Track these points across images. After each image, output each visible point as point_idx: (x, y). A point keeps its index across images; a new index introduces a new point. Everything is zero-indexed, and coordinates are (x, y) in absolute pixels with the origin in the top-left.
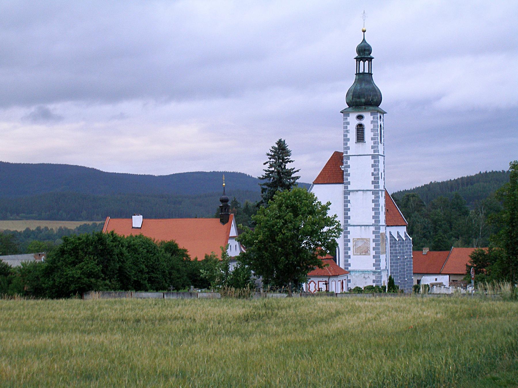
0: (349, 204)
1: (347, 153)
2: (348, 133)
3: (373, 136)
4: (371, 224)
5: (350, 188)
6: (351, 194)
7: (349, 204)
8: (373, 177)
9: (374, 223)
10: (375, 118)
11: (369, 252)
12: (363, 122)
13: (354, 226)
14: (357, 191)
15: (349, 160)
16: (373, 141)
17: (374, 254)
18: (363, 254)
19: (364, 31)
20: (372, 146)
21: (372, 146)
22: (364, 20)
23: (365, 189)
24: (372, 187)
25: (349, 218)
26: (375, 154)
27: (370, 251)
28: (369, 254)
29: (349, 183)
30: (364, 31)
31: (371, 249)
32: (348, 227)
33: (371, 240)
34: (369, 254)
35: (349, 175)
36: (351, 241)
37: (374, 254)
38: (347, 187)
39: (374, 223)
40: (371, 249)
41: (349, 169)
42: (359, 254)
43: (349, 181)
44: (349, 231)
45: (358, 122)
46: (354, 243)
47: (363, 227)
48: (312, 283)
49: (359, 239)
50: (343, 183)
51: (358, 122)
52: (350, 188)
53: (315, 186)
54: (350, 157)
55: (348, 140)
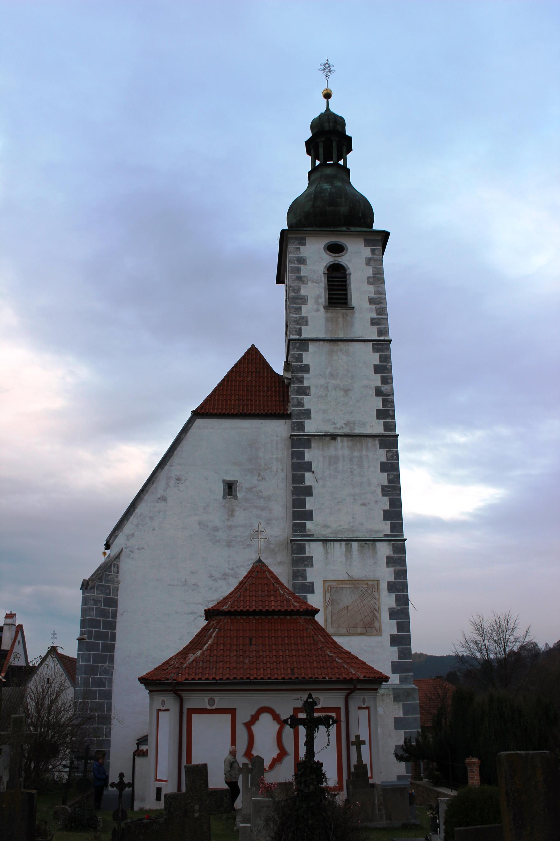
0: (308, 475)
1: (300, 334)
2: (304, 283)
3: (373, 295)
4: (381, 536)
5: (310, 427)
6: (313, 445)
7: (308, 475)
8: (380, 399)
9: (388, 532)
10: (377, 252)
11: (377, 624)
12: (344, 260)
13: (325, 541)
14: (333, 437)
15: (307, 350)
16: (374, 307)
17: (395, 632)
18: (359, 630)
19: (327, 96)
20: (372, 319)
21: (372, 319)
22: (327, 76)
23: (358, 430)
24: (378, 428)
25: (309, 515)
26: (382, 338)
27: (379, 620)
28: (379, 633)
29: (307, 414)
30: (327, 96)
31: (385, 615)
32: (307, 544)
33: (384, 586)
34: (379, 633)
35: (305, 391)
36: (319, 588)
37: (395, 632)
38: (301, 426)
39: (388, 532)
40: (385, 615)
41: (305, 375)
42: (344, 631)
43: (306, 407)
44: (311, 558)
45: (328, 259)
46: (328, 595)
47: (355, 545)
48: (266, 718)
49: (342, 581)
50: (284, 415)
51: (328, 259)
52: (310, 427)
53: (199, 422)
54: (310, 343)
55: (304, 300)
